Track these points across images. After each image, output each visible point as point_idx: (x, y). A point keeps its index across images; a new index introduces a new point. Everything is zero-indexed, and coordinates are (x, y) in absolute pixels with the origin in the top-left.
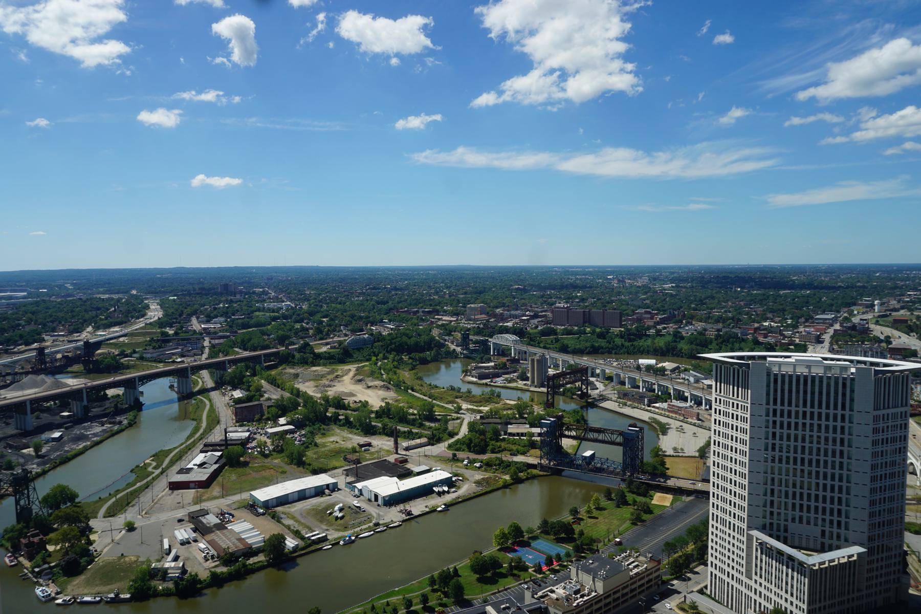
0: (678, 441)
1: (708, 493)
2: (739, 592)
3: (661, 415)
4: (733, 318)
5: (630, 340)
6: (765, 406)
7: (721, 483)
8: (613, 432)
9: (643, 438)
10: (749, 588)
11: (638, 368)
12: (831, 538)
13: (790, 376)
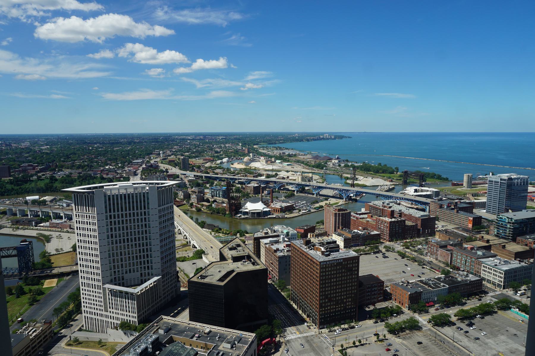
0: (59, 243)
1: (78, 271)
2: (102, 321)
3: (45, 230)
4: (88, 166)
5: (18, 185)
6: (105, 214)
7: (84, 263)
8: (8, 249)
9: (32, 248)
10: (107, 316)
11: (26, 203)
12: (145, 276)
13: (117, 195)
